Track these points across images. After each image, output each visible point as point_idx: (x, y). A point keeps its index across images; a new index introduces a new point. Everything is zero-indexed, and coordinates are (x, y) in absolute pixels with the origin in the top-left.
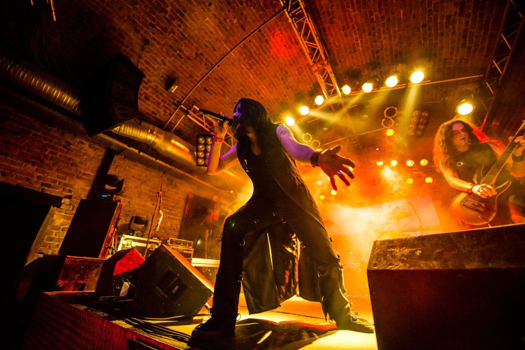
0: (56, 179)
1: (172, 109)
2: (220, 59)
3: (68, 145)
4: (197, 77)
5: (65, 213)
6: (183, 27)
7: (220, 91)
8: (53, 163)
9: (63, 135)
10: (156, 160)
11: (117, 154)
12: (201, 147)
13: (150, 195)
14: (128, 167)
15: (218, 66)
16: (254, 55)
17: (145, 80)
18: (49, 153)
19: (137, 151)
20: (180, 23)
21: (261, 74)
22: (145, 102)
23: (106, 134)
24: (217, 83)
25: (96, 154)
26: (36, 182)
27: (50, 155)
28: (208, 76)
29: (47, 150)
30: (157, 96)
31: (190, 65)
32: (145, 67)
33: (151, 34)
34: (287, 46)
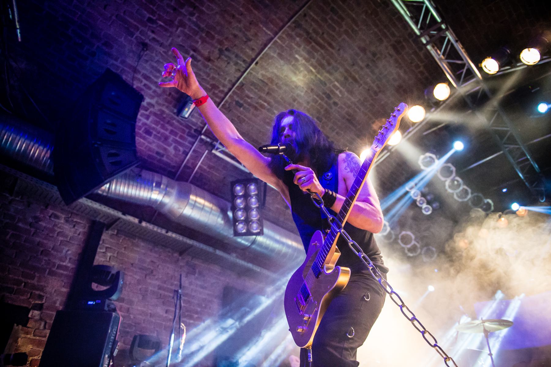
0: (20, 278)
1: (187, 143)
2: (257, 51)
3: (37, 222)
4: (224, 86)
5: (34, 336)
6: (197, 15)
7: (263, 102)
9: (29, 206)
10: (167, 232)
11: (107, 229)
12: (239, 201)
13: (161, 295)
14: (123, 249)
15: (257, 63)
16: (314, 35)
17: (144, 103)
19: (136, 221)
20: (191, 9)
21: (329, 64)
22: (144, 138)
23: (89, 197)
24: (256, 91)
25: (75, 233)
28: (241, 82)
30: (163, 127)
31: (211, 69)
32: (143, 84)
33: (150, 33)
34: (370, 12)
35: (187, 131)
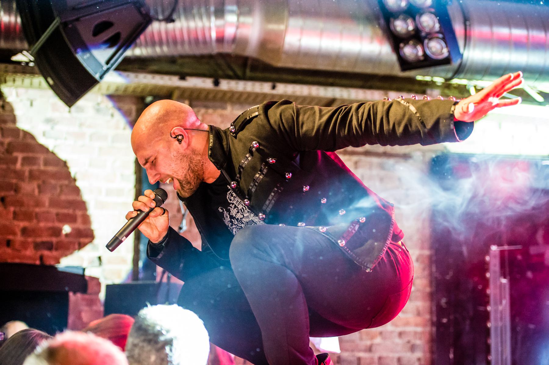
8: (39, 187)
10: (274, 87)
18: (22, 164)
26: (24, 245)
27: (27, 169)
29: (15, 160)
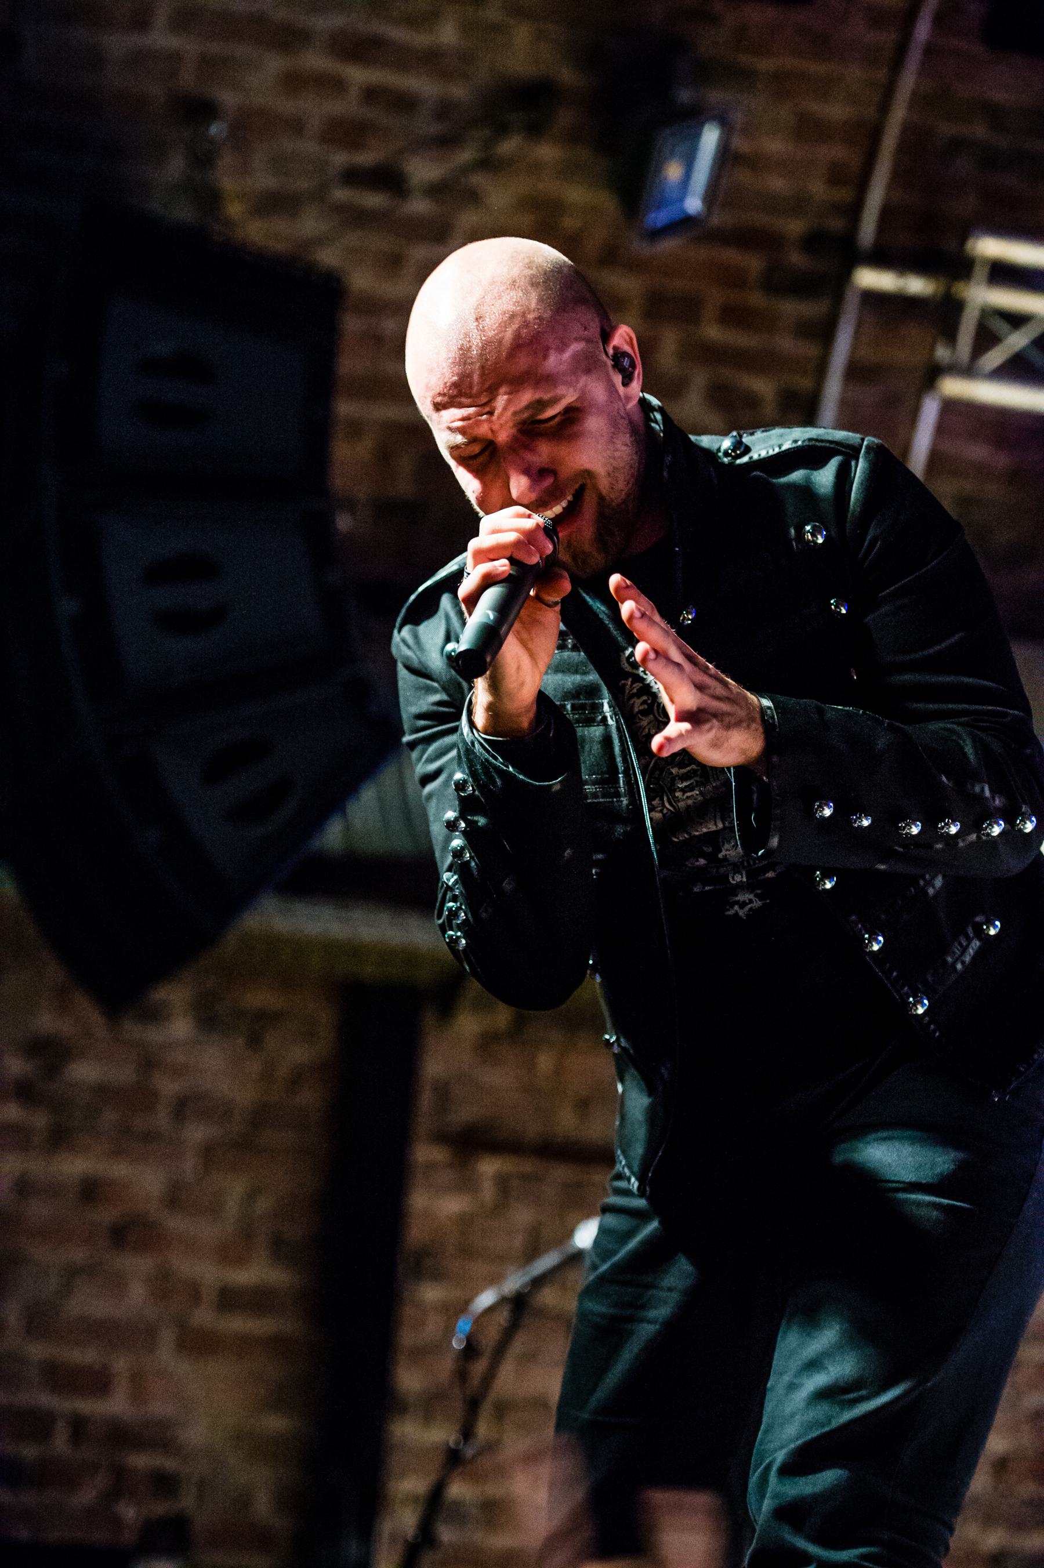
1: (787, 344)
35: (754, 263)
